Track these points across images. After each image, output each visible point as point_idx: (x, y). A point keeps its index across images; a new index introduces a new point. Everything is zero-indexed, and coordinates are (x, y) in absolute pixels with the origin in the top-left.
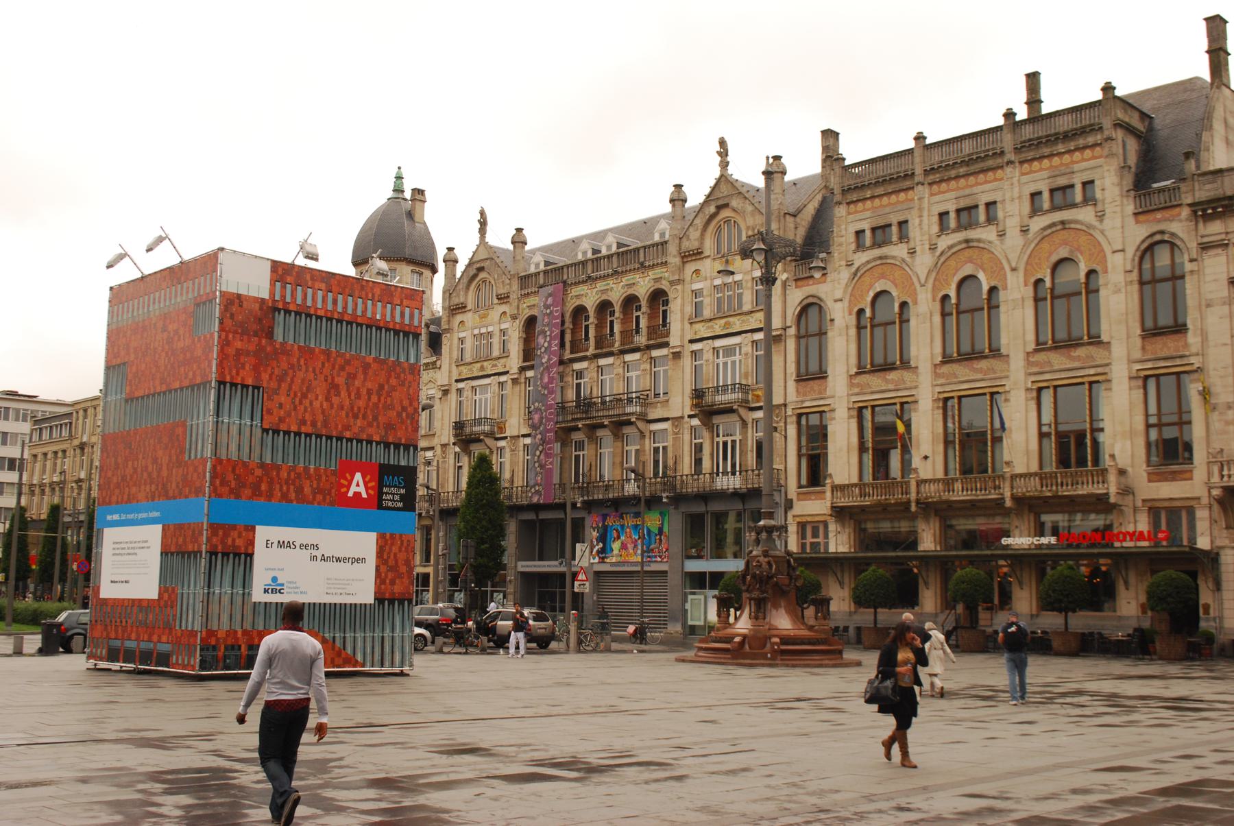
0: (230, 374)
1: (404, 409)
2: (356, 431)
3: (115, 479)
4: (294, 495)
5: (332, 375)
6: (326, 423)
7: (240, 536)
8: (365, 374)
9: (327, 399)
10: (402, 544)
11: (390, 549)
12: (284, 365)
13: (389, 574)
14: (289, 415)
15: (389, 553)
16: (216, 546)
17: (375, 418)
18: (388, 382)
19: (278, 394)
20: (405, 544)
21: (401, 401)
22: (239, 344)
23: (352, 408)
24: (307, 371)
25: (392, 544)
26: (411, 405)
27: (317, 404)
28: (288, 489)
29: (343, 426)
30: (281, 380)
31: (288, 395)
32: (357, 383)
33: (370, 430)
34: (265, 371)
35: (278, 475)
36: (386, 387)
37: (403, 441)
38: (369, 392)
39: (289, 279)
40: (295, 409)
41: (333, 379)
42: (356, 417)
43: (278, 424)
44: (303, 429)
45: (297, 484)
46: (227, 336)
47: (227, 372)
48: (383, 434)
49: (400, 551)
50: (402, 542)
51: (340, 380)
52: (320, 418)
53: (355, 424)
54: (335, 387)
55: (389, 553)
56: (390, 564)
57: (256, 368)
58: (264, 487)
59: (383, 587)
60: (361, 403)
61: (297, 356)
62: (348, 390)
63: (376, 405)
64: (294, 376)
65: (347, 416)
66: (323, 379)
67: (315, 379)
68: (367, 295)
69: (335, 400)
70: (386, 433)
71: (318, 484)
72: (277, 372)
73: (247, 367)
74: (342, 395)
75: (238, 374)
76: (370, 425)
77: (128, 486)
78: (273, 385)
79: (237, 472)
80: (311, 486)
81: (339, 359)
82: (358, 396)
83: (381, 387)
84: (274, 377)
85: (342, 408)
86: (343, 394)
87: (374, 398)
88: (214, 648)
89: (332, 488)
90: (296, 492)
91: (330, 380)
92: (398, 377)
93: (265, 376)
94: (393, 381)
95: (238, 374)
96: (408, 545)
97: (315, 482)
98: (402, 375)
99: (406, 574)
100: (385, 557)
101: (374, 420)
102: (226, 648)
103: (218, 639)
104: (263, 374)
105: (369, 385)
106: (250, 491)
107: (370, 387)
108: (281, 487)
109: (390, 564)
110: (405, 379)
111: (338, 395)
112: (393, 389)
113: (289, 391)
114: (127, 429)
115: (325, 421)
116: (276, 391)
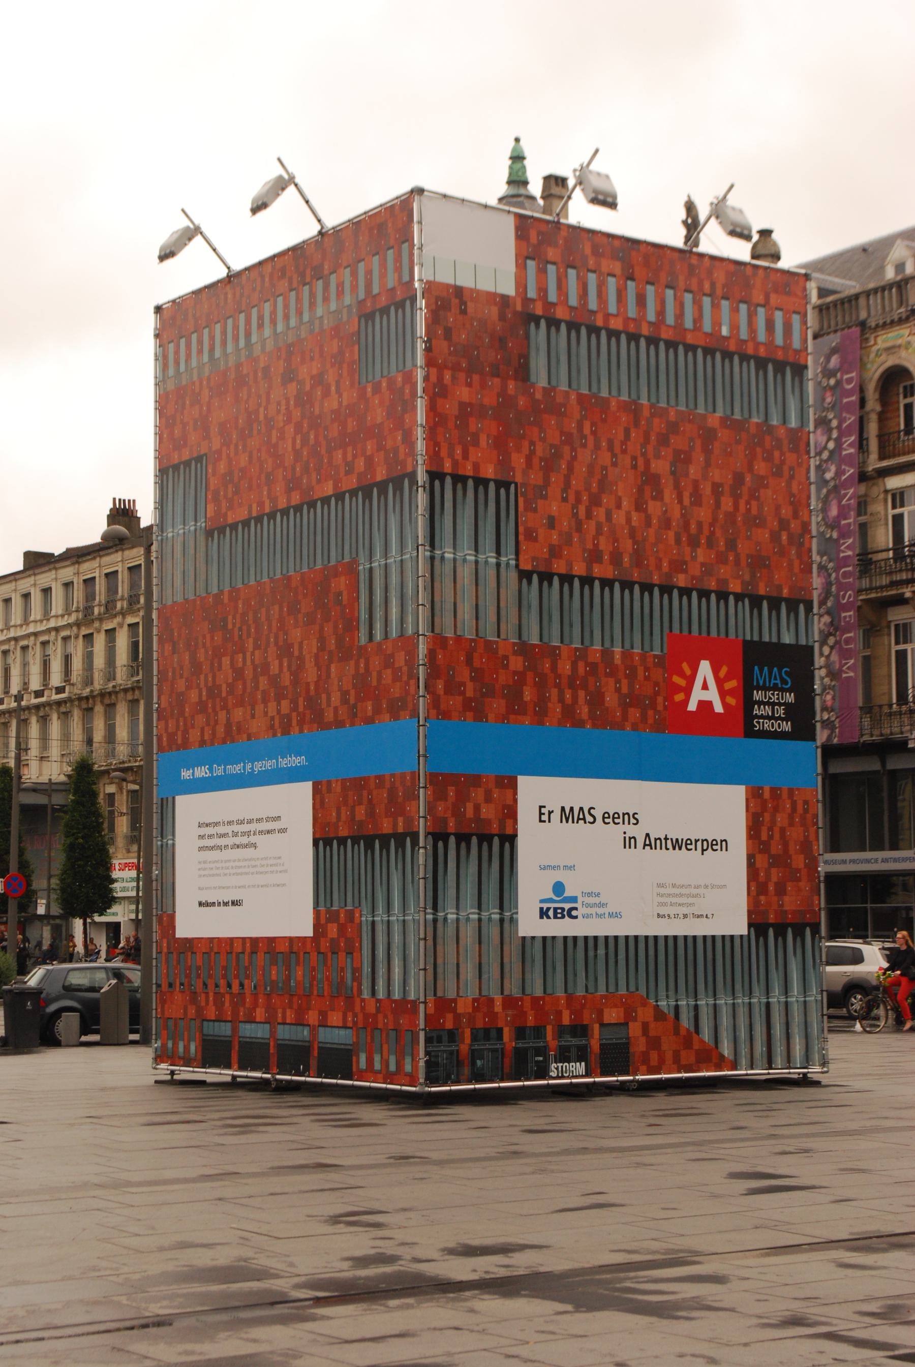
0: (451, 455)
1: (784, 524)
2: (697, 573)
3: (193, 696)
4: (586, 710)
5: (643, 454)
6: (638, 559)
8: (707, 451)
9: (639, 506)
11: (773, 821)
13: (774, 871)
14: (567, 540)
15: (770, 829)
16: (445, 821)
17: (731, 544)
18: (750, 469)
19: (545, 498)
20: (800, 810)
21: (778, 508)
22: (464, 393)
23: (686, 525)
24: (597, 447)
25: (776, 809)
26: (796, 515)
27: (619, 517)
28: (575, 698)
29: (671, 563)
30: (549, 466)
31: (565, 500)
32: (694, 471)
33: (724, 571)
34: (518, 449)
35: (554, 667)
37: (785, 592)
39: (551, 253)
40: (579, 528)
41: (647, 463)
42: (694, 543)
44: (597, 571)
46: (440, 378)
47: (444, 453)
48: (747, 577)
49: (791, 824)
50: (794, 804)
51: (660, 466)
52: (627, 545)
53: (694, 559)
54: (650, 480)
55: (770, 829)
56: (774, 851)
57: (500, 444)
59: (763, 899)
60: (703, 514)
61: (577, 416)
62: (677, 486)
63: (731, 517)
64: (574, 458)
65: (678, 541)
66: (628, 461)
67: (614, 464)
69: (654, 508)
70: (753, 575)
71: (631, 686)
72: (539, 451)
73: (483, 441)
75: (465, 455)
76: (721, 559)
77: (225, 707)
78: (535, 478)
79: (477, 663)
80: (618, 690)
81: (656, 421)
82: (697, 500)
83: (738, 479)
84: (536, 461)
85: (667, 524)
86: (669, 494)
87: (727, 504)
88: (452, 1036)
90: (589, 703)
91: (641, 467)
92: (769, 459)
93: (518, 461)
94: (761, 467)
95: (465, 455)
96: (806, 811)
97: (625, 682)
98: (777, 454)
100: (764, 837)
102: (474, 1038)
103: (457, 1017)
105: (716, 475)
106: (503, 702)
107: (717, 479)
109: (774, 851)
110: (783, 462)
111: (659, 497)
112: (761, 482)
114: (215, 591)
115: (636, 551)
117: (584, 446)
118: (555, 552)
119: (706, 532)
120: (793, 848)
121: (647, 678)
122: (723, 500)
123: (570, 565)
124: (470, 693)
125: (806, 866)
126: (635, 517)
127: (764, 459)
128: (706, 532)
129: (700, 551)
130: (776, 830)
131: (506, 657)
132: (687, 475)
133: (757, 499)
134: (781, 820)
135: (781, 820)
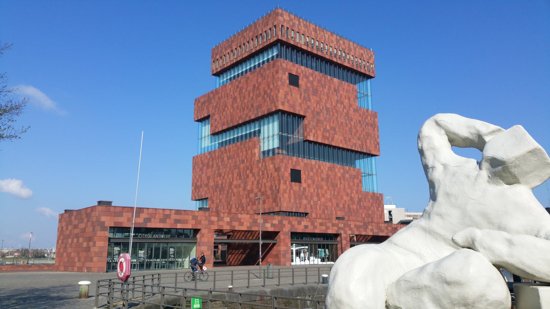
1: (265, 92)
4: (221, 163)
7: (203, 191)
8: (247, 83)
9: (232, 107)
11: (262, 181)
12: (217, 99)
15: (261, 184)
17: (252, 105)
20: (270, 177)
21: (264, 88)
25: (263, 178)
26: (269, 88)
27: (228, 112)
32: (244, 91)
36: (257, 85)
42: (244, 109)
45: (222, 157)
48: (256, 113)
49: (267, 182)
53: (243, 114)
58: (210, 163)
60: (246, 101)
62: (240, 98)
64: (220, 103)
65: (240, 112)
68: (247, 39)
69: (235, 105)
70: (257, 111)
74: (238, 101)
76: (250, 111)
78: (213, 111)
79: (202, 160)
80: (227, 156)
83: (254, 86)
87: (251, 95)
89: (235, 154)
90: (221, 162)
92: (262, 76)
96: (271, 176)
97: (228, 153)
99: (271, 196)
100: (260, 187)
101: (251, 107)
105: (249, 89)
108: (216, 161)
110: (266, 74)
113: (218, 111)
115: (231, 119)
116: (214, 115)
117: (222, 98)
118: (216, 127)
119: (246, 105)
120: (268, 189)
121: (233, 151)
122: (250, 94)
123: (219, 129)
124: (201, 167)
125: (271, 193)
126: (231, 110)
127: (261, 77)
128: (246, 105)
129: (245, 111)
130: (263, 184)
131: (207, 156)
132: (242, 93)
133: (259, 89)
134: (265, 181)
135: (265, 181)
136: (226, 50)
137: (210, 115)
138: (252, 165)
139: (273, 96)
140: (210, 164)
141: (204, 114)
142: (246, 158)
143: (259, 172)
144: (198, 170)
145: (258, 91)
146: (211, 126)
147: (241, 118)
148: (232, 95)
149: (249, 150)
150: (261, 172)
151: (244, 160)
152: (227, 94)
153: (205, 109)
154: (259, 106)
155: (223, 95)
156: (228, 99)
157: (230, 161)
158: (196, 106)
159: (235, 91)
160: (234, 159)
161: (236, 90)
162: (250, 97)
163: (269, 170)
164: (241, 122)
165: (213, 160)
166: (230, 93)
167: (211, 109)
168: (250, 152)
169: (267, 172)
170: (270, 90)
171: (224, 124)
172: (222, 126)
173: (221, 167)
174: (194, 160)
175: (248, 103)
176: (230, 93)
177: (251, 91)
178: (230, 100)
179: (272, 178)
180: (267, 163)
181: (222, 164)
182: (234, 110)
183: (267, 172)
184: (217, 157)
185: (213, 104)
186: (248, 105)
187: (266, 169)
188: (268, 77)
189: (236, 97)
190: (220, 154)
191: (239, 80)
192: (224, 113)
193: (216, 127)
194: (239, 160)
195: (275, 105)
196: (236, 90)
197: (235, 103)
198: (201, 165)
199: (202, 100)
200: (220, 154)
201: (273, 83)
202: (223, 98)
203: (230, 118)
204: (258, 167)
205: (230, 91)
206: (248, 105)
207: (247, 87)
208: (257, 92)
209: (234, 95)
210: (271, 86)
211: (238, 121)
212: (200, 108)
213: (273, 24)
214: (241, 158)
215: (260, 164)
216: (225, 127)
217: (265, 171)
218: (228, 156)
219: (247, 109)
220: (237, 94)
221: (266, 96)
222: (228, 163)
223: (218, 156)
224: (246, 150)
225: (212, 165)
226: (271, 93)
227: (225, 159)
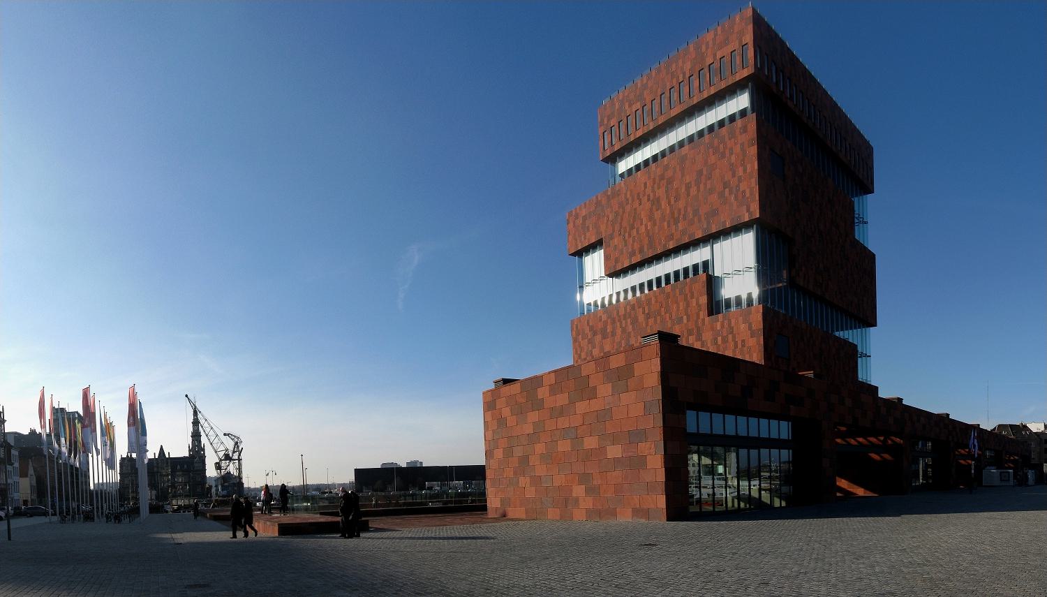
1: (726, 185)
9: (651, 218)
10: (736, 347)
20: (740, 346)
24: (633, 200)
32: (675, 185)
38: (688, 187)
42: (676, 221)
43: (615, 266)
48: (705, 226)
50: (736, 343)
60: (681, 204)
64: (624, 212)
66: (646, 197)
69: (657, 215)
70: (708, 223)
74: (663, 207)
80: (643, 313)
83: (700, 173)
94: (712, 159)
104: (602, 226)
105: (688, 179)
113: (620, 231)
116: (612, 238)
118: (617, 261)
119: (682, 212)
121: (656, 302)
122: (691, 190)
128: (682, 212)
136: (630, 106)
137: (602, 239)
138: (700, 325)
139: (744, 192)
140: (608, 331)
141: (589, 239)
142: (687, 314)
143: (716, 339)
144: (584, 343)
145: (709, 182)
146: (607, 258)
147: (672, 239)
148: (649, 196)
149: (692, 297)
150: (720, 338)
151: (682, 317)
152: (638, 194)
153: (591, 229)
154: (714, 213)
155: (628, 196)
156: (640, 204)
157: (651, 321)
158: (571, 225)
159: (656, 186)
160: (659, 317)
161: (659, 185)
162: (691, 195)
163: (738, 334)
164: (671, 245)
165: (614, 322)
166: (644, 191)
167: (603, 228)
168: (694, 300)
169: (734, 337)
170: (736, 178)
171: (633, 254)
172: (630, 258)
173: (632, 334)
174: (575, 326)
175: (686, 208)
176: (644, 191)
177: (693, 183)
178: (648, 205)
179: (745, 349)
180: (733, 321)
181: (634, 329)
182: (655, 224)
183: (734, 337)
184: (622, 317)
185: (608, 217)
186: (686, 211)
187: (732, 333)
188: (731, 154)
189: (659, 198)
190: (628, 310)
191: (666, 163)
192: (634, 232)
193: (617, 261)
194: (670, 318)
195: (748, 210)
196: (659, 185)
197: (657, 210)
198: (589, 334)
199: (584, 212)
200: (628, 310)
201: (743, 165)
202: (630, 202)
203: (646, 241)
204: (712, 329)
205: (645, 187)
206: (686, 211)
207: (683, 175)
208: (705, 184)
209: (655, 195)
210: (740, 172)
211: (665, 245)
212: (580, 228)
213: (741, 41)
214: (674, 314)
215: (719, 324)
216: (635, 260)
217: (730, 336)
218: (646, 312)
219: (684, 219)
220: (661, 192)
221: (727, 190)
222: (647, 325)
223: (625, 315)
224: (686, 299)
225: (612, 332)
226: (738, 186)
227: (641, 318)
